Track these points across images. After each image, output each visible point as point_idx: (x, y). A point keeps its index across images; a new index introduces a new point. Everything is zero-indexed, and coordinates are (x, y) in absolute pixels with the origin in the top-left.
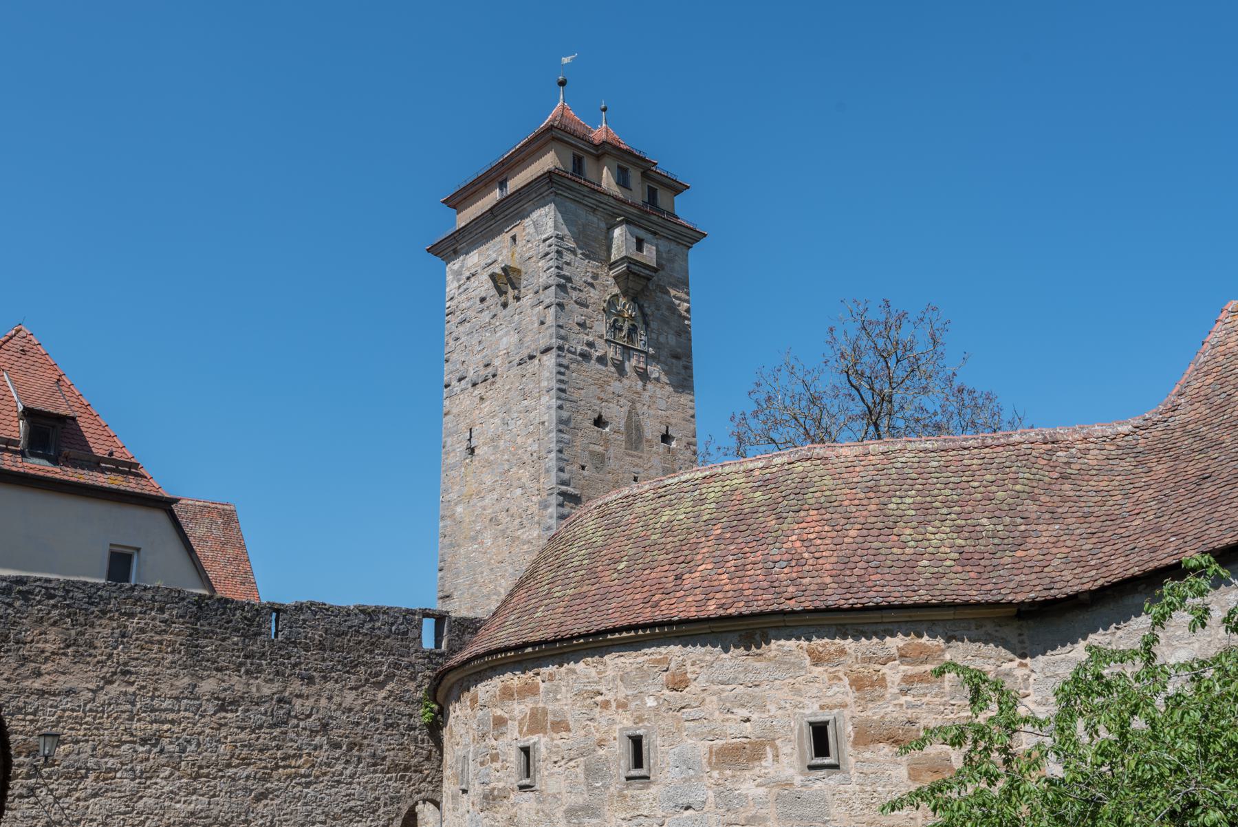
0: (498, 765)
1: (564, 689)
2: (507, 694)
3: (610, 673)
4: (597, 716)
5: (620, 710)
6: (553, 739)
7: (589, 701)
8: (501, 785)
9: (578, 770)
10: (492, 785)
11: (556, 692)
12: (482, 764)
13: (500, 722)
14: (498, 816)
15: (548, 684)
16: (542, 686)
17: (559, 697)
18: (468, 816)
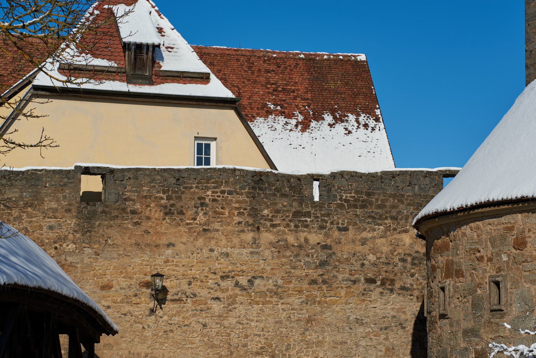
5: (489, 263)
17: (458, 253)
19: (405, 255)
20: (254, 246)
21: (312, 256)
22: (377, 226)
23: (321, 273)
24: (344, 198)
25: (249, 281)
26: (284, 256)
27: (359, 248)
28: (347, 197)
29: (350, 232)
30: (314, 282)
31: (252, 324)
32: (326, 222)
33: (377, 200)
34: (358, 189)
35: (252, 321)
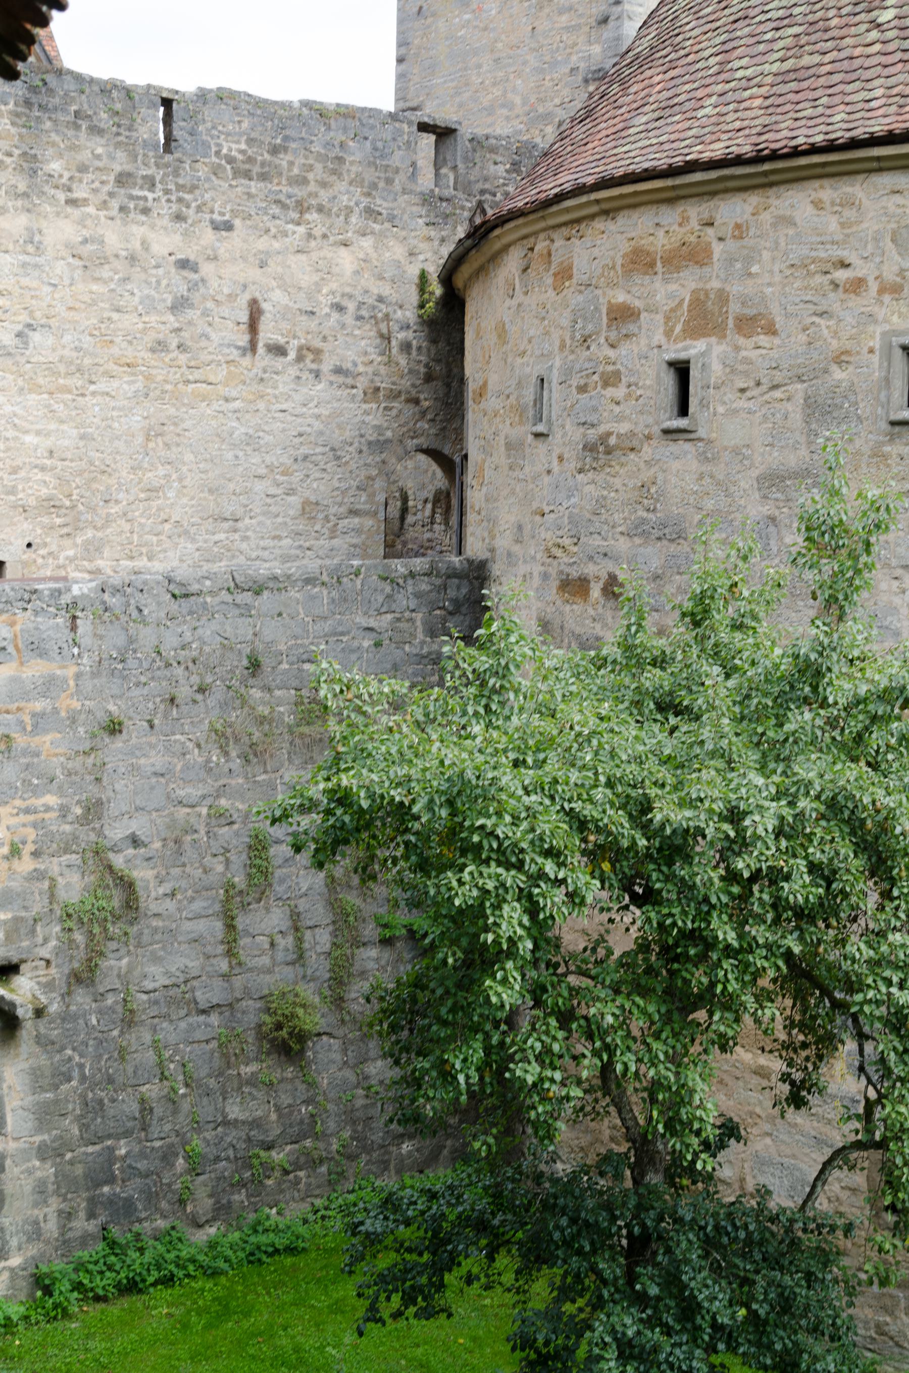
0: (620, 392)
1: (766, 255)
2: (641, 262)
3: (870, 226)
4: (836, 307)
5: (887, 298)
6: (737, 349)
7: (819, 279)
8: (624, 428)
9: (789, 406)
10: (602, 429)
11: (749, 261)
12: (582, 389)
13: (622, 315)
14: (617, 482)
15: (731, 245)
16: (718, 249)
17: (755, 269)
18: (547, 479)
19: (343, 295)
20: (30, 248)
21: (158, 282)
22: (290, 226)
23: (177, 325)
24: (225, 151)
25: (19, 335)
26: (97, 280)
27: (254, 273)
28: (230, 150)
29: (234, 234)
30: (160, 346)
31: (29, 439)
32: (188, 207)
33: (291, 163)
34: (253, 135)
35: (27, 432)
